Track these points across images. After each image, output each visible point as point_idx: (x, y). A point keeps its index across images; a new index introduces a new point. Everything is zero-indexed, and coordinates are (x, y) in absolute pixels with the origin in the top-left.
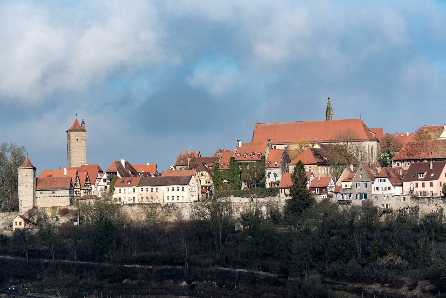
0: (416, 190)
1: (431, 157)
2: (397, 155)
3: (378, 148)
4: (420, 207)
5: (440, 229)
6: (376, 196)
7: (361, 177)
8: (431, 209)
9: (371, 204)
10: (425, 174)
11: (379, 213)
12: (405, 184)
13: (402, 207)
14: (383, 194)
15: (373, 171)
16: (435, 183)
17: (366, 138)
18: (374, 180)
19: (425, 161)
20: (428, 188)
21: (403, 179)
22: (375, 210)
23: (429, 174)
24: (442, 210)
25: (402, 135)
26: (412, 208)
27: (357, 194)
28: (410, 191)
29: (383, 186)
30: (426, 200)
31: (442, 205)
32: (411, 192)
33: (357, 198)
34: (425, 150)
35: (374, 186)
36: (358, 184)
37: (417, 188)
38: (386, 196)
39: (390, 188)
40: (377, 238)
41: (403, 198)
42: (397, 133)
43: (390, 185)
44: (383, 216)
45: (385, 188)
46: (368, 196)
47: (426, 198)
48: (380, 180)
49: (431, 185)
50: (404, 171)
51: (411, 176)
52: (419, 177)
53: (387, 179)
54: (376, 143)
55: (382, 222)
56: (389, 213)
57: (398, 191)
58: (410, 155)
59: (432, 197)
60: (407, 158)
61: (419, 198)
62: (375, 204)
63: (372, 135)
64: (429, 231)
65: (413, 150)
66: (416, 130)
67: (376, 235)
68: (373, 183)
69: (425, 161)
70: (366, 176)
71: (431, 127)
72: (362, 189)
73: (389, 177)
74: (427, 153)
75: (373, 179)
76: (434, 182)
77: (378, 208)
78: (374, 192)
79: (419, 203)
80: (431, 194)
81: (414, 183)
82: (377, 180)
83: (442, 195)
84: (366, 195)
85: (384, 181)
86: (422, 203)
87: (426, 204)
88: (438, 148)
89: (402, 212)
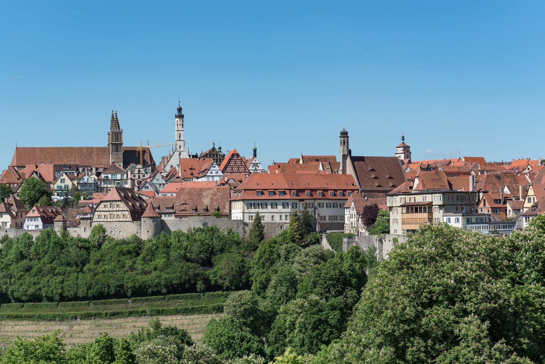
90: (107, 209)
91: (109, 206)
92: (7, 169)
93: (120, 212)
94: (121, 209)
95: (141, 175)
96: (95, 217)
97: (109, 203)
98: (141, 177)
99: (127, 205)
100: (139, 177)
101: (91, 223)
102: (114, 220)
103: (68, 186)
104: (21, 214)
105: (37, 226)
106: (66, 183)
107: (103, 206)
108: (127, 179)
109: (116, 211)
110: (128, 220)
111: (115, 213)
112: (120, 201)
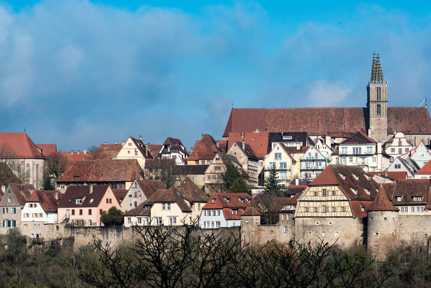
0: (72, 218)
1: (101, 179)
2: (63, 176)
3: (44, 167)
4: (75, 238)
5: (92, 265)
6: (25, 223)
7: (9, 200)
8: (88, 241)
9: (18, 233)
10: (84, 199)
11: (28, 244)
12: (60, 210)
13: (55, 238)
14: (34, 221)
15: (23, 194)
16: (95, 210)
17: (31, 155)
18: (24, 205)
19: (85, 184)
20: (86, 217)
21: (58, 203)
22: (24, 240)
23: (87, 200)
24: (100, 242)
25: (78, 153)
26: (66, 239)
27: (4, 221)
28: (66, 219)
29: (34, 213)
30: (82, 230)
31: (100, 237)
32: (67, 220)
33: (4, 226)
34: (95, 172)
35: (24, 211)
36: (5, 209)
37: (73, 216)
38: (37, 224)
39: (41, 215)
40: (18, 274)
41: (56, 227)
42: (73, 151)
43: (42, 211)
44: (33, 247)
45: (36, 214)
46: (17, 223)
47: (82, 227)
48: (31, 205)
49: (90, 212)
50: (60, 194)
51: (67, 201)
52: (77, 202)
53: (38, 204)
54: (42, 161)
55: (29, 256)
56: (39, 244)
57: (52, 218)
58: (77, 176)
59: (89, 227)
60: (73, 180)
61: (74, 227)
62: (24, 233)
63: (37, 152)
64: (79, 268)
65: (81, 171)
66: (90, 147)
67: (17, 270)
68: (22, 208)
69: (85, 184)
70: (15, 198)
71: (113, 145)
72: (10, 215)
73: (41, 201)
74: (96, 174)
75: (22, 203)
76: (94, 209)
77: (28, 238)
78: (23, 219)
79: (74, 233)
80: (90, 223)
81: (71, 209)
82: (27, 204)
83: (103, 225)
84: (14, 222)
85: (35, 207)
86: (78, 233)
87: (82, 235)
88: (110, 169)
89: (54, 244)
90: (318, 198)
91: (321, 194)
92: (200, 138)
93: (337, 203)
94: (338, 199)
95: (403, 149)
96: (300, 210)
97: (320, 189)
98: (404, 152)
99: (347, 191)
100: (400, 150)
101: (294, 219)
102: (328, 214)
103: (285, 164)
104: (199, 204)
105: (219, 223)
106: (283, 161)
107: (312, 194)
108: (376, 154)
109: (331, 201)
110: (348, 215)
111: (329, 203)
112: (337, 185)
